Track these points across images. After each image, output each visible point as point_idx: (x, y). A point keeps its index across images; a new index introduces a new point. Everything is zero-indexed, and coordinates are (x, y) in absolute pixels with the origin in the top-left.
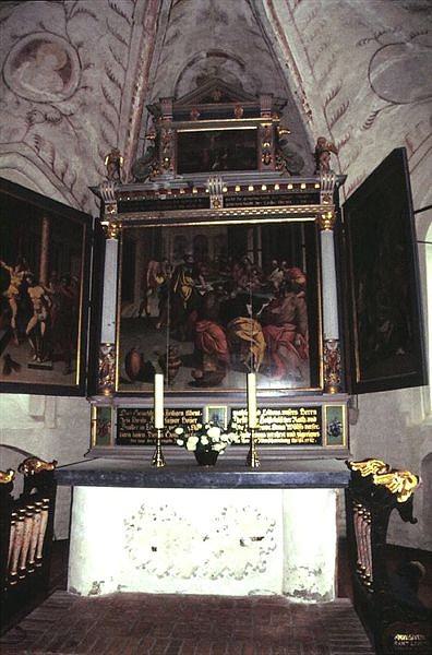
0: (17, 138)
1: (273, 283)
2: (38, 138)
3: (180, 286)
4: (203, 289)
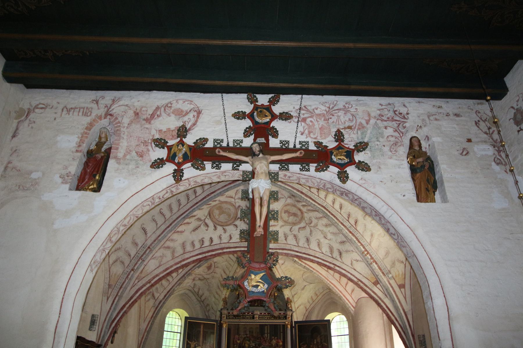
1: (272, 344)
3: (245, 344)
4: (252, 345)
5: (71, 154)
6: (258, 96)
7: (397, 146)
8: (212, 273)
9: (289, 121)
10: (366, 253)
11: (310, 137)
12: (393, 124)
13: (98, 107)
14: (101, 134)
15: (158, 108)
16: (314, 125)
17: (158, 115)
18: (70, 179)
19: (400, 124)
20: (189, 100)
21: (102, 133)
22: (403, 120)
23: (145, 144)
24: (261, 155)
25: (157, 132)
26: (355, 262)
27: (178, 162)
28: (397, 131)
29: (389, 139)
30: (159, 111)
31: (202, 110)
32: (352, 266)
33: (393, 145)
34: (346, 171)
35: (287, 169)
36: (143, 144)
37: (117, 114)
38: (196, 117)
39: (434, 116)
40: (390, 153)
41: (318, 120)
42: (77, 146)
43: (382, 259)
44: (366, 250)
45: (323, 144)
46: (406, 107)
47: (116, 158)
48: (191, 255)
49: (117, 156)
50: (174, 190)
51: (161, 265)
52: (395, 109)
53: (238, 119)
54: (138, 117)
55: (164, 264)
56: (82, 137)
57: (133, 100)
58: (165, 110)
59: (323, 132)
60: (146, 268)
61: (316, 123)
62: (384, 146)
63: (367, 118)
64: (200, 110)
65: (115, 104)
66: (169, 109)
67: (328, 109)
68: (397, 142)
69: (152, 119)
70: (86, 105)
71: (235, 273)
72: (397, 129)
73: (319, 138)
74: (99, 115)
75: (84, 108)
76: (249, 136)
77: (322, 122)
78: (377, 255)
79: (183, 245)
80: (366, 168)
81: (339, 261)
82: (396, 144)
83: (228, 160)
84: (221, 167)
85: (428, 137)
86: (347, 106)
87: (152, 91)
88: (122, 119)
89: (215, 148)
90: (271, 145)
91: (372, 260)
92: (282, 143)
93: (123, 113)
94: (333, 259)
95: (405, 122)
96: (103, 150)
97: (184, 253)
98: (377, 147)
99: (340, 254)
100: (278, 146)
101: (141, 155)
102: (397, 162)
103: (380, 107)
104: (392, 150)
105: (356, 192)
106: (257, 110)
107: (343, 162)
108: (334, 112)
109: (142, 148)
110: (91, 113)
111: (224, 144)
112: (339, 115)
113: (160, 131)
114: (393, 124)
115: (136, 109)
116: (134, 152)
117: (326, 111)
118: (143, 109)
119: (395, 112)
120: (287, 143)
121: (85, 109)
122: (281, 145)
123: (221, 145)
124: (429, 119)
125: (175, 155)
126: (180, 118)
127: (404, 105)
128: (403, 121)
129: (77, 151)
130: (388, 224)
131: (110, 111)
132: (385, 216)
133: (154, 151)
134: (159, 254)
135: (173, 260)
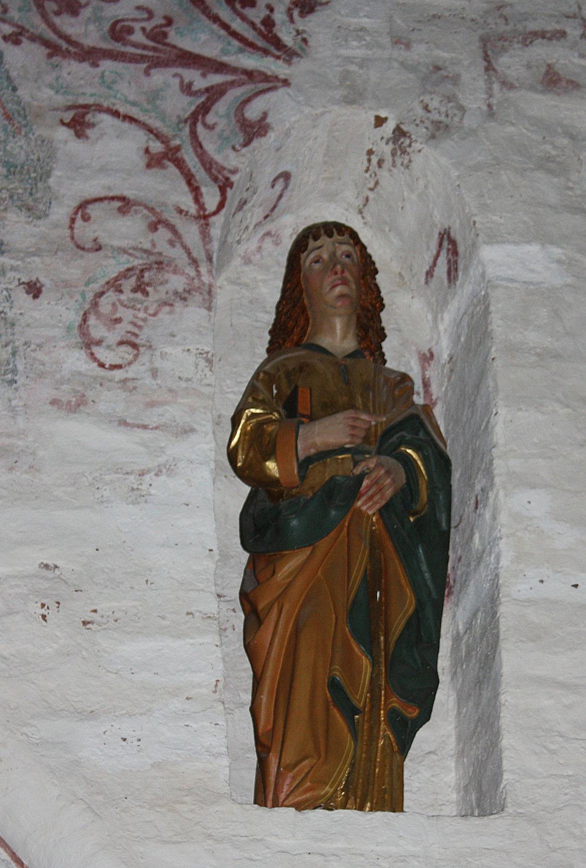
7: (155, 295)
12: (154, 96)
19: (214, 94)
22: (250, 61)
28: (180, 164)
29: (86, 232)
33: (115, 285)
39: (541, 51)
62: (34, 290)
72: (182, 139)
85: (453, 242)
95: (272, 83)
104: (97, 329)
114: (154, 96)
124: (489, 68)
128: (250, 75)
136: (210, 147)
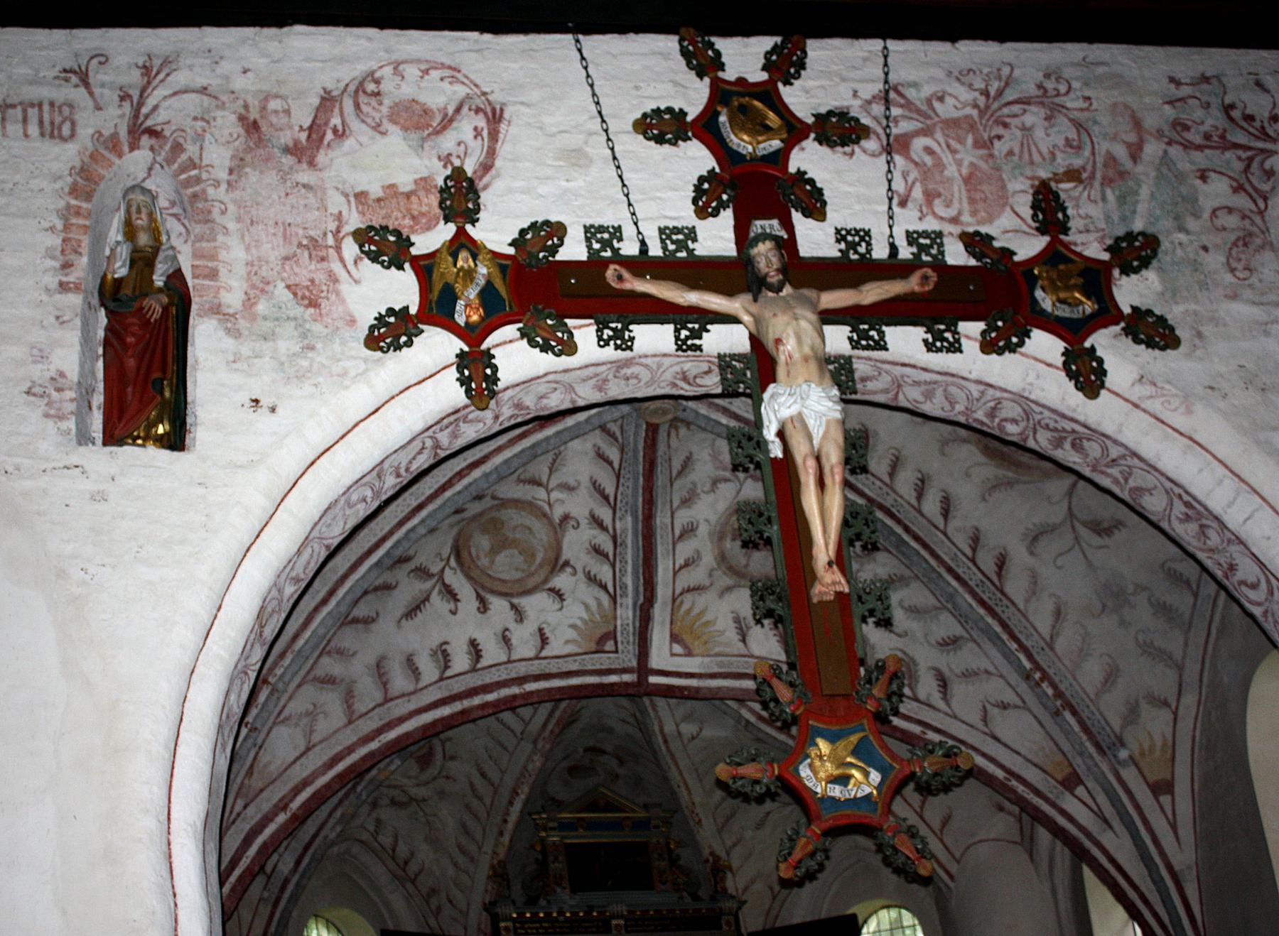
0: (357, 822)
2: (378, 822)
5: (44, 297)
6: (721, 43)
7: (1252, 247)
8: (435, 778)
9: (847, 149)
10: (1037, 676)
11: (934, 214)
12: (1228, 163)
13: (95, 101)
14: (134, 216)
15: (328, 101)
16: (939, 165)
17: (335, 131)
18: (72, 400)
19: (1251, 160)
20: (443, 66)
21: (139, 212)
22: (1260, 145)
23: (314, 253)
24: (787, 290)
25: (349, 201)
26: (996, 711)
27: (467, 323)
28: (1245, 191)
29: (1219, 222)
30: (336, 111)
31: (504, 104)
32: (986, 725)
33: (1235, 244)
34: (1093, 349)
35: (881, 345)
36: (306, 254)
37: (174, 128)
38: (485, 133)
40: (1229, 278)
41: (953, 143)
42: (57, 264)
43: (1093, 696)
44: (1038, 667)
45: (996, 244)
46: (1267, 91)
47: (216, 310)
48: (412, 706)
49: (220, 305)
50: (444, 438)
51: (314, 746)
52: (1228, 100)
53: (660, 140)
54: (260, 138)
55: (321, 742)
56: (67, 227)
57: (225, 67)
58: (357, 106)
59: (978, 196)
60: (264, 758)
61: (947, 158)
62: (1205, 249)
63: (1132, 138)
64: (498, 107)
65: (154, 84)
66: (373, 101)
67: (982, 101)
68: (1250, 234)
69: (318, 148)
70: (45, 93)
71: (522, 775)
72: (1243, 180)
73: (966, 218)
74: (106, 133)
75: (40, 105)
76: (715, 214)
77: (969, 155)
78: (1074, 683)
79: (380, 670)
80: (1163, 337)
81: (939, 710)
82: (1244, 240)
83: (657, 311)
84: (632, 339)
86: (1050, 85)
87: (291, 24)
88: (201, 148)
89: (595, 264)
90: (805, 250)
91: (1059, 703)
92: (843, 239)
93: (200, 124)
94: (915, 704)
96: (159, 281)
97: (387, 700)
98: (1179, 252)
99: (944, 684)
100: (831, 250)
101: (310, 299)
102: (1256, 312)
103: (1173, 91)
104: (1234, 264)
105: (1120, 431)
106: (726, 103)
107: (1076, 314)
108: (1006, 111)
109: (306, 270)
110: (73, 124)
111: (629, 248)
112: (1028, 124)
113: (361, 196)
114: (1228, 163)
115: (246, 107)
116: (281, 285)
117: (976, 106)
118: (274, 105)
119: (1227, 109)
120: (862, 239)
121: (46, 108)
122: (843, 246)
123: (616, 251)
125: (449, 297)
126: (424, 140)
127: (1259, 84)
128: (1262, 151)
129: (63, 287)
130: (1234, 549)
131: (147, 117)
132: (1225, 519)
133: (357, 282)
134: (297, 706)
135: (351, 727)
136: (1255, 182)
